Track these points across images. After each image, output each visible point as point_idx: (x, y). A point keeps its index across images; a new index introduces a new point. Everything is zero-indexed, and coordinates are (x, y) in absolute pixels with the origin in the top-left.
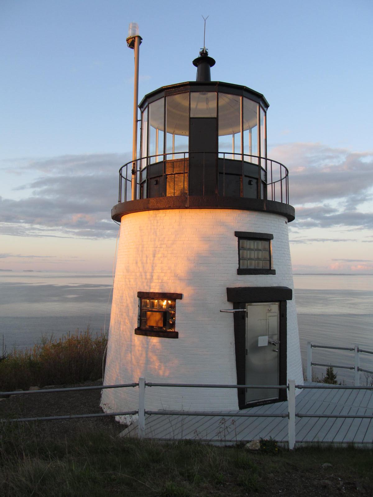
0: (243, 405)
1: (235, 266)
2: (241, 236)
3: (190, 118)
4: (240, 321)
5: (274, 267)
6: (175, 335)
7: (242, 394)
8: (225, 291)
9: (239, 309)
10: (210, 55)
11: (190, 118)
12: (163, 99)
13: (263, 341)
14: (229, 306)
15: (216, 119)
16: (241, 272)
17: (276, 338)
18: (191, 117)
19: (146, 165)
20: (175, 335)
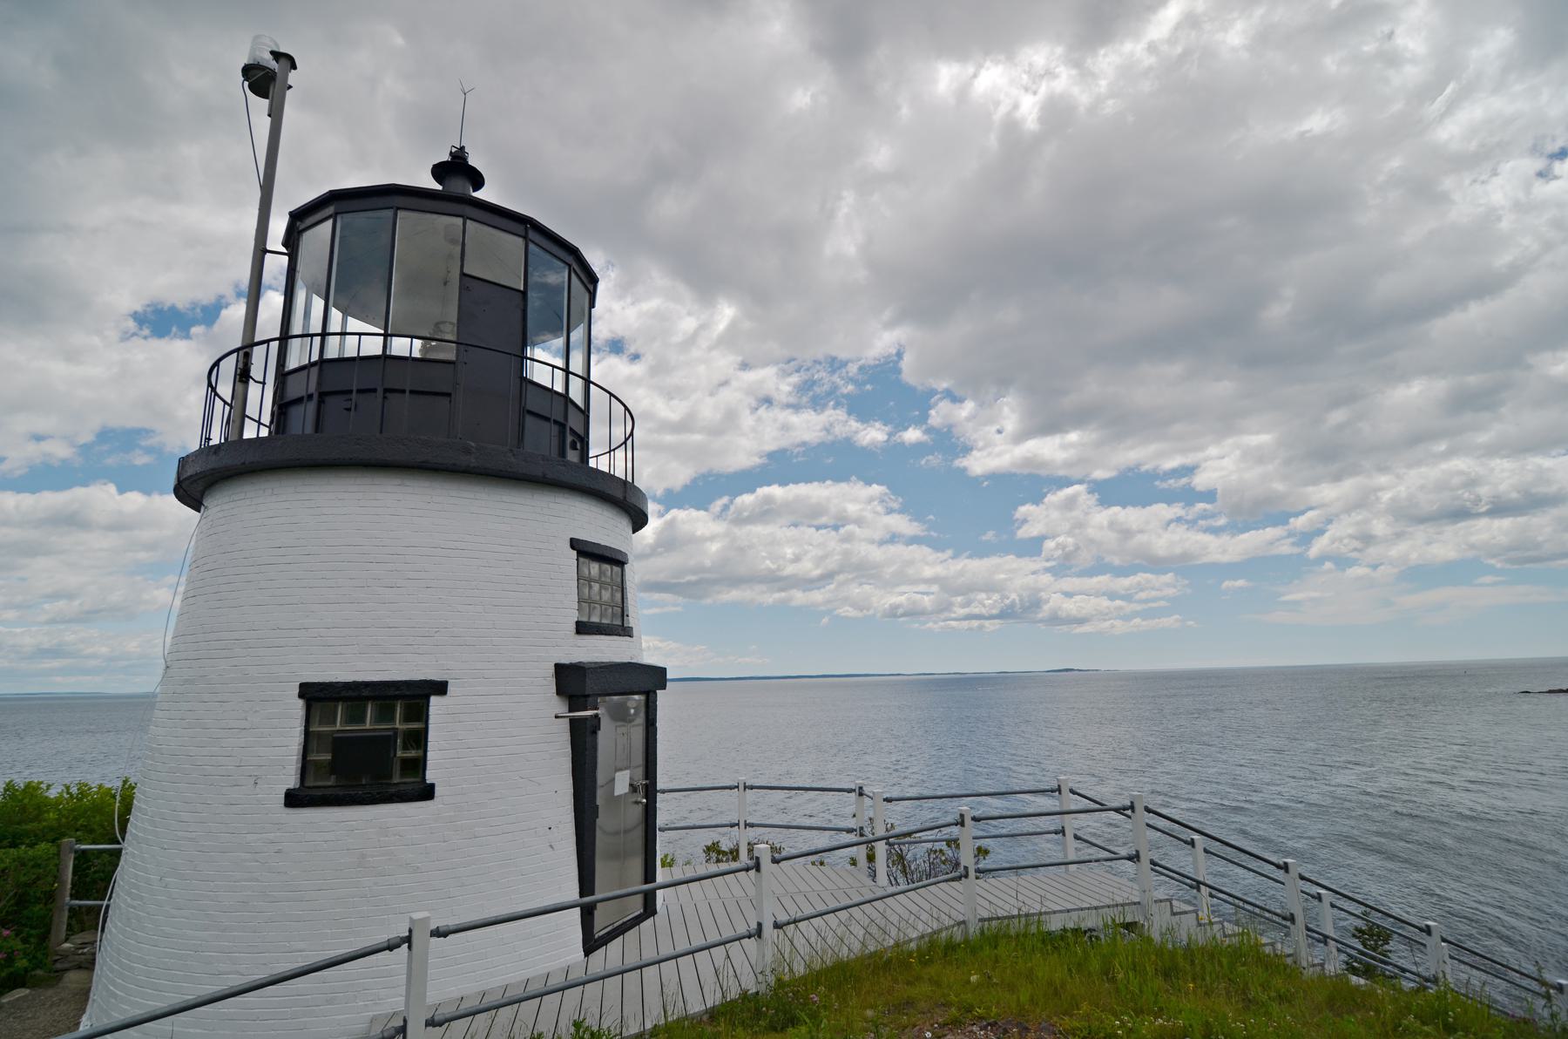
0: (591, 945)
1: (574, 616)
2: (585, 551)
3: (463, 275)
4: (583, 739)
5: (632, 621)
6: (427, 793)
7: (588, 913)
8: (552, 670)
9: (586, 709)
10: (472, 162)
11: (463, 275)
12: (330, 223)
13: (622, 785)
14: (560, 707)
15: (524, 293)
16: (582, 628)
17: (640, 772)
18: (466, 271)
19: (315, 358)
20: (427, 793)
